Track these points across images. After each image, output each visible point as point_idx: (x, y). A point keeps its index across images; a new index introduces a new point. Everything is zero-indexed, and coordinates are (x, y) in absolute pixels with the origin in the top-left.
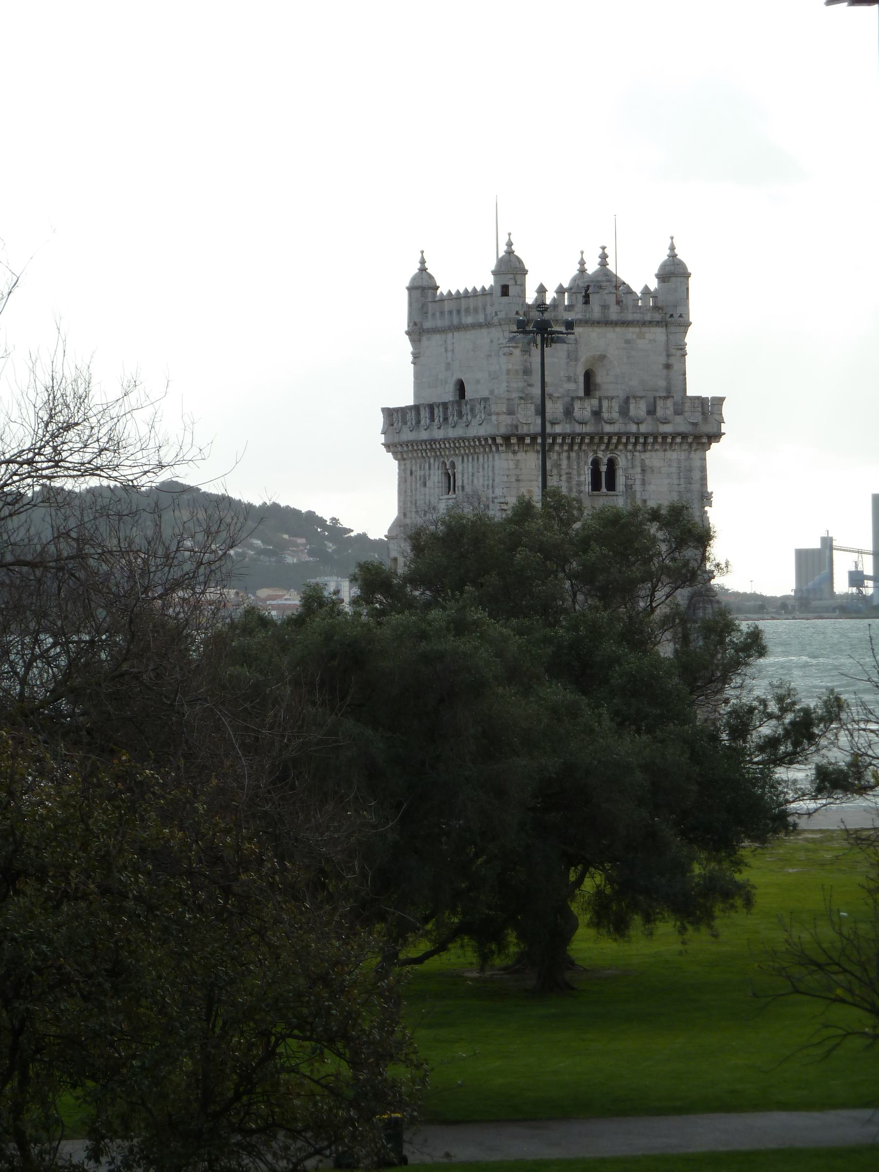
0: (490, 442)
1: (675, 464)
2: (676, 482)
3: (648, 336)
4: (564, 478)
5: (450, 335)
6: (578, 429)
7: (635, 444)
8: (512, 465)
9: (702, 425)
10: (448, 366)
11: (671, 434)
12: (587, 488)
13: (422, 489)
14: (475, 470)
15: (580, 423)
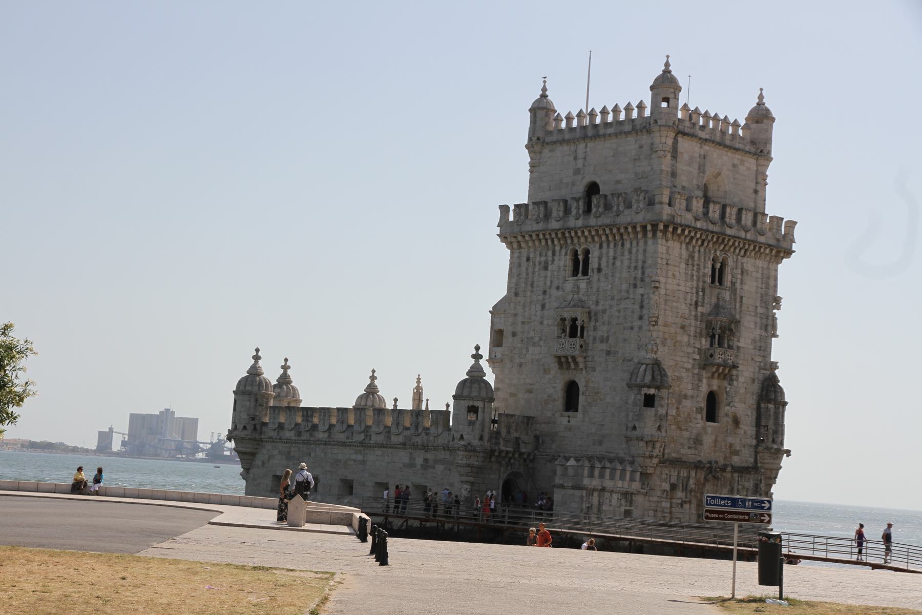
0: (649, 227)
1: (760, 271)
2: (760, 286)
3: (747, 164)
4: (695, 268)
5: (581, 146)
6: (711, 227)
7: (740, 251)
8: (664, 250)
9: (778, 244)
10: (577, 172)
11: (765, 244)
12: (709, 280)
13: (543, 273)
14: (619, 253)
15: (713, 223)
